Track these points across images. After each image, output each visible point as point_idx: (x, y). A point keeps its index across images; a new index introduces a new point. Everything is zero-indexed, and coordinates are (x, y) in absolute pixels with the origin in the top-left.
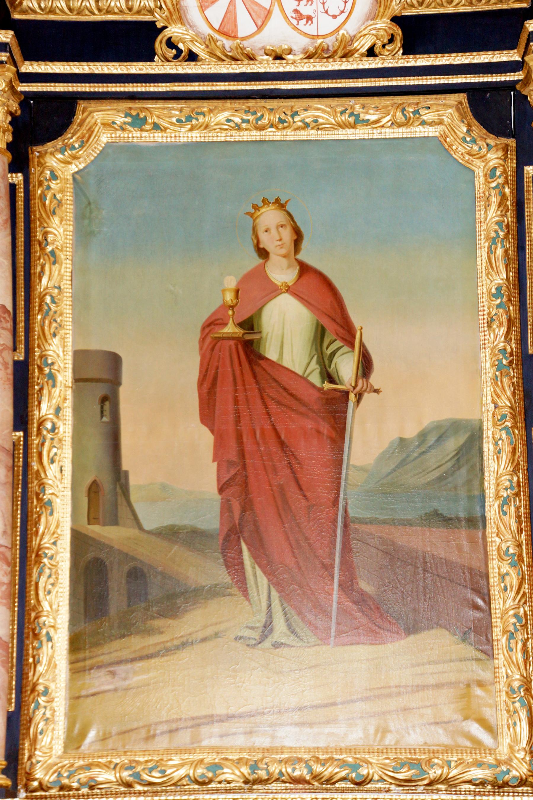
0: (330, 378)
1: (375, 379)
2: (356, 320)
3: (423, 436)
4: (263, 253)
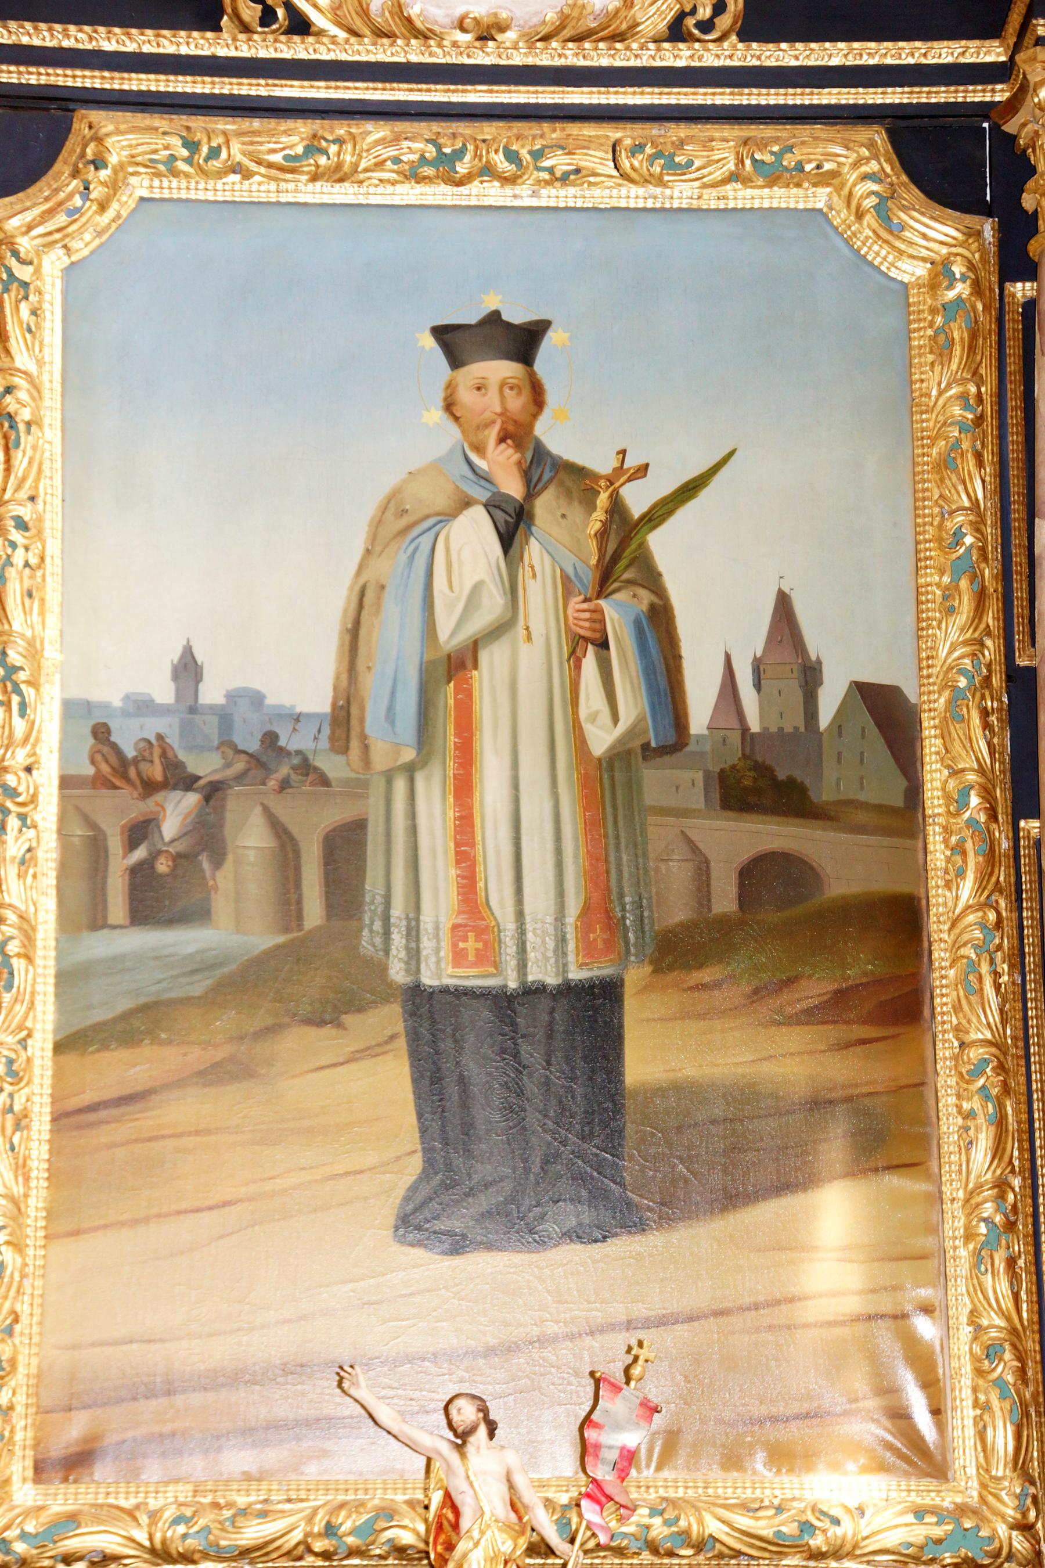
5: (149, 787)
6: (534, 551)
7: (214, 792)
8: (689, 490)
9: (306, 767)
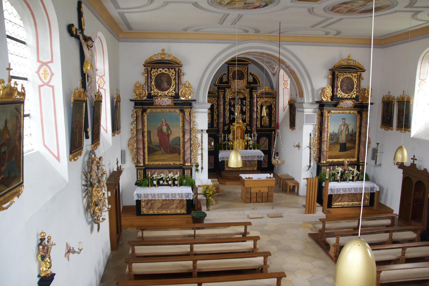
0: (168, 133)
2: (170, 128)
3: (175, 138)
4: (163, 122)
6: (345, 127)
7: (334, 136)
9: (337, 135)
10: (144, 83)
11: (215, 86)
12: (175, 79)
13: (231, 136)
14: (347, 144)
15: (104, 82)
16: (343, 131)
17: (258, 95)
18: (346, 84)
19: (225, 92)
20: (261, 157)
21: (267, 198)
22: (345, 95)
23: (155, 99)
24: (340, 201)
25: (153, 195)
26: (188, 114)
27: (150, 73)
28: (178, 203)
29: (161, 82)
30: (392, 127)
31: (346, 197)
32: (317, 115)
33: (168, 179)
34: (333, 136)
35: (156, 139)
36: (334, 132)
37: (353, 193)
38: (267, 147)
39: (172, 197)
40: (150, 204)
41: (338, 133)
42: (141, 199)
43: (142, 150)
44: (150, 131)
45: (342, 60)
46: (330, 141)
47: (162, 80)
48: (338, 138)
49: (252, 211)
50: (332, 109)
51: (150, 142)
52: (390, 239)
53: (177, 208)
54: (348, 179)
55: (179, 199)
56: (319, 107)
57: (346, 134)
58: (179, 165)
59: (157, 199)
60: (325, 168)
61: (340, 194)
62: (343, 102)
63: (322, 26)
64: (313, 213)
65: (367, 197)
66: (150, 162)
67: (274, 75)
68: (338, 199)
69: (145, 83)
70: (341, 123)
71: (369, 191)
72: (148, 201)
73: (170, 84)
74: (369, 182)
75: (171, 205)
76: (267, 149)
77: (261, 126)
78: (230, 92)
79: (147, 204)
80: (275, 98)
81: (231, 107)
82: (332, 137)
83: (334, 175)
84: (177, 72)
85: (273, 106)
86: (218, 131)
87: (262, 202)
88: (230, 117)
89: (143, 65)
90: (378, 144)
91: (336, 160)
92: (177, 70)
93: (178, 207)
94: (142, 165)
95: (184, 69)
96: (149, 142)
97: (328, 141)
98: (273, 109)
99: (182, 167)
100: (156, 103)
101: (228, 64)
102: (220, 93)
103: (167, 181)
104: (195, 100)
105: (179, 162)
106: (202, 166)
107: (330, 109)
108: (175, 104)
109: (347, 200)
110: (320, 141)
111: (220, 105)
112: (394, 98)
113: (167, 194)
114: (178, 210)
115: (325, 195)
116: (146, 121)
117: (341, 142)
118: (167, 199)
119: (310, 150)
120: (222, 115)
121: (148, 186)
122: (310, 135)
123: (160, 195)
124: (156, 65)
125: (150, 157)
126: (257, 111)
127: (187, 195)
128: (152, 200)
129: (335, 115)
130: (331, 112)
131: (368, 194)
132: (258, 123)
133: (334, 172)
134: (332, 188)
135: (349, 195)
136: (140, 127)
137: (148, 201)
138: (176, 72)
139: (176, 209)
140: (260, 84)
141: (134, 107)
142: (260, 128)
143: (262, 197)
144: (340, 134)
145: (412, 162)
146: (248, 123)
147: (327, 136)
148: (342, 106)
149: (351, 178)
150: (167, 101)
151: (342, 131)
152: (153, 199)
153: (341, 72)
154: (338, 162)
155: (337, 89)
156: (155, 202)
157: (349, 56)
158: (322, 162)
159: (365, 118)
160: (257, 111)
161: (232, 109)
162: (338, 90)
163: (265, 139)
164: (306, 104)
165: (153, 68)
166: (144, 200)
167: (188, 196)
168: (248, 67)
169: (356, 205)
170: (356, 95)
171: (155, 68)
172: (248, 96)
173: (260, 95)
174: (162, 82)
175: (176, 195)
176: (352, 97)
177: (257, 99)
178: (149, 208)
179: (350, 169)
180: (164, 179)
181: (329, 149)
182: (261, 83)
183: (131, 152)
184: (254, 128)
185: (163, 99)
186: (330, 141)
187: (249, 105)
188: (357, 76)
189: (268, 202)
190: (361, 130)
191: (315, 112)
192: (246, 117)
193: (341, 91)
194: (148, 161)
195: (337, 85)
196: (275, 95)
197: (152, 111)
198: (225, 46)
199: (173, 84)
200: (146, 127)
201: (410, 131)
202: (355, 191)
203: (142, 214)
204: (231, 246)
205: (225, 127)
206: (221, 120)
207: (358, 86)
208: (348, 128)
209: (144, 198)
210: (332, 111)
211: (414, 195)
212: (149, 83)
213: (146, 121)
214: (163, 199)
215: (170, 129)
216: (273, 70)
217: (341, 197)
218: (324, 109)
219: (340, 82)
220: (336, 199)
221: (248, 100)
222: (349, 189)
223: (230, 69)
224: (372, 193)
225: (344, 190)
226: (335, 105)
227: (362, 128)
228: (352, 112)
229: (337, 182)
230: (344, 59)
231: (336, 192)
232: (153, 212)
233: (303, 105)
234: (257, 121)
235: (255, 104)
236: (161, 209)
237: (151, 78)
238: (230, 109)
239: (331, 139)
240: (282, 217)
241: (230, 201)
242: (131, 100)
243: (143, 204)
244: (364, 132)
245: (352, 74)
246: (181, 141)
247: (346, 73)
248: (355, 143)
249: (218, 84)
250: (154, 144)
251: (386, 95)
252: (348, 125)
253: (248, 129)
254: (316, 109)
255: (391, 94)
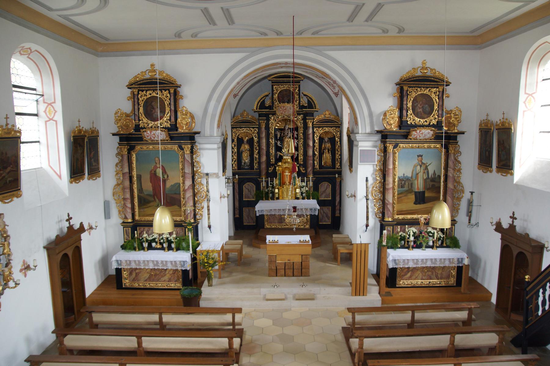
1: (169, 178)
2: (167, 171)
3: (174, 184)
4: (156, 163)
5: (402, 181)
6: (422, 168)
8: (430, 164)
9: (410, 180)
10: (131, 111)
11: (255, 112)
12: (170, 104)
13: (276, 182)
14: (426, 192)
15: (54, 112)
16: (419, 174)
17: (314, 123)
18: (421, 105)
19: (268, 120)
20: (315, 210)
21: (301, 270)
22: (419, 121)
23: (144, 132)
24: (410, 278)
25: (137, 262)
26: (188, 152)
27: (137, 96)
28: (171, 274)
29: (152, 110)
30: (491, 167)
31: (419, 272)
32: (377, 152)
33: (162, 241)
34: (404, 182)
35: (148, 187)
36: (405, 176)
37: (430, 267)
38: (331, 196)
39: (162, 266)
40: (134, 275)
41: (412, 177)
42: (122, 267)
43: (129, 201)
44: (141, 176)
45: (412, 69)
46: (399, 189)
47: (153, 106)
48: (412, 184)
49: (272, 289)
50: (400, 141)
51: (140, 190)
52: (451, 346)
53: (170, 280)
54: (424, 245)
55: (171, 269)
56: (382, 139)
57: (425, 178)
58: (180, 221)
59: (143, 268)
60: (391, 228)
61: (408, 268)
62: (416, 130)
63: (365, 18)
64: (363, 295)
65: (452, 273)
66: (141, 218)
67: (336, 94)
68: (406, 274)
69: (132, 110)
70: (416, 161)
71: (455, 264)
72: (131, 271)
73: (163, 111)
74: (458, 249)
75: (162, 276)
76: (330, 199)
77: (321, 166)
78: (276, 121)
79: (131, 274)
80: (339, 127)
81: (277, 141)
82: (401, 183)
83: (403, 238)
84: (172, 95)
85: (337, 139)
86: (259, 174)
87: (293, 276)
88: (276, 155)
89: (127, 86)
90: (472, 193)
91: (409, 217)
92: (172, 91)
93: (172, 279)
94: (130, 220)
95: (184, 91)
96: (139, 190)
97: (396, 188)
98: (337, 143)
99: (182, 224)
100: (145, 137)
101: (272, 82)
102: (260, 121)
103: (161, 244)
104: (199, 133)
105: (179, 218)
106: (209, 223)
107: (398, 141)
108: (172, 138)
109: (421, 277)
110: (383, 189)
111: (262, 138)
112: (492, 123)
113: (156, 261)
114: (172, 284)
115: (382, 268)
116: (134, 162)
117: (416, 190)
118: (156, 268)
119: (367, 201)
120: (265, 152)
121: (135, 249)
122: (367, 180)
123: (146, 262)
124: (144, 86)
125: (142, 210)
126: (314, 146)
127: (182, 263)
128: (136, 269)
129: (406, 150)
130: (400, 146)
131: (454, 269)
132: (316, 162)
133: (405, 234)
134: (397, 259)
135: (423, 269)
136: (126, 170)
137: (132, 271)
138: (171, 95)
139: (168, 282)
140: (316, 109)
141: (119, 144)
142: (319, 169)
143: (293, 269)
144: (414, 178)
145: (511, 223)
146: (302, 163)
147: (394, 182)
148: (416, 137)
149: (431, 243)
150: (160, 135)
151: (417, 174)
152: (138, 268)
153: (412, 87)
154: (412, 219)
155: (407, 112)
156: (141, 272)
157: (423, 63)
158: (386, 219)
159: (452, 155)
160: (314, 146)
161: (279, 143)
162: (408, 114)
163: (327, 184)
164: (360, 135)
165: (141, 90)
166: (127, 269)
167: (184, 265)
168: (299, 86)
169: (435, 284)
170: (437, 120)
171: (143, 91)
172: (301, 124)
173: (318, 123)
174: (154, 108)
175: (168, 263)
176: (431, 124)
177: (313, 129)
178: (134, 280)
179: (428, 231)
180: (156, 240)
181: (397, 201)
182: (317, 107)
183: (116, 203)
184: (310, 169)
185: (154, 132)
186: (399, 189)
187: (302, 138)
188: (438, 92)
189: (302, 276)
190: (447, 172)
191: (375, 147)
192: (298, 155)
193: (413, 115)
194: (139, 216)
195: (407, 107)
196: (340, 123)
197: (142, 148)
198: (237, 56)
199: (167, 111)
200: (135, 170)
201: (512, 174)
202: (434, 263)
203: (124, 287)
204: (200, 343)
205: (270, 169)
206: (264, 159)
207: (440, 107)
208: (428, 169)
209: (126, 265)
210: (401, 145)
211: (515, 274)
212: (135, 110)
213: (134, 162)
214: (151, 268)
215: (166, 173)
216: (334, 88)
217: (411, 271)
218: (386, 141)
219: (411, 102)
220: (403, 275)
221: (301, 131)
222: (422, 260)
223: (274, 89)
224: (459, 266)
225: (433, 260)
226: (406, 136)
227: (449, 169)
228: (432, 145)
229: (407, 250)
230: (416, 67)
231: (403, 265)
232: (139, 285)
233: (356, 136)
234: (314, 160)
235: (311, 136)
236: (149, 281)
237: (139, 104)
238: (276, 144)
239: (401, 186)
240: (313, 299)
241: (251, 273)
242: (114, 135)
243: (126, 274)
244: (451, 175)
245: (429, 90)
246: (182, 190)
247: (420, 87)
248: (439, 192)
249: (257, 109)
250: (146, 193)
251: (484, 120)
252: (427, 165)
253: (302, 171)
254: (376, 141)
255: (489, 118)
